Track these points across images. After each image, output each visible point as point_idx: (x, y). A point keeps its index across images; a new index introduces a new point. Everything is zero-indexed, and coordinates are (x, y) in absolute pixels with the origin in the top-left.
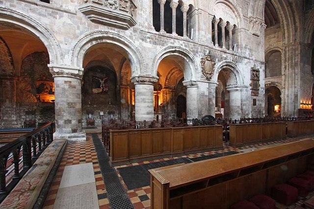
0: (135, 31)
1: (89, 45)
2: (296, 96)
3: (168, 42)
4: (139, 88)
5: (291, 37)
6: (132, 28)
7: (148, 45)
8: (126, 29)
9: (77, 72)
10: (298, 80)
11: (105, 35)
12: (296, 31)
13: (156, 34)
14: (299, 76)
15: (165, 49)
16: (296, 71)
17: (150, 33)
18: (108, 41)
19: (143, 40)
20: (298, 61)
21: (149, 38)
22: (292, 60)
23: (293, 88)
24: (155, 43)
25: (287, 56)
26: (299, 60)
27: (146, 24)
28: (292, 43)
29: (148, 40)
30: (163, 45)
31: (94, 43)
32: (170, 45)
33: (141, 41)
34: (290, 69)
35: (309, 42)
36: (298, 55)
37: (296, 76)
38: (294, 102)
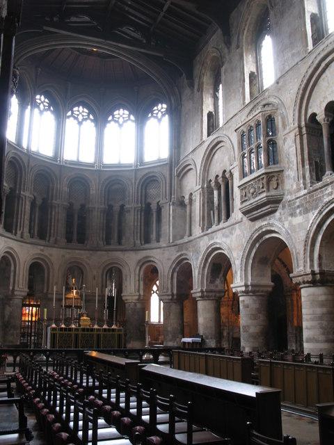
0: (284, 207)
1: (254, 251)
3: (323, 196)
4: (305, 293)
6: (281, 206)
7: (298, 220)
8: (276, 210)
9: (243, 289)
11: (260, 232)
13: (305, 195)
15: (320, 212)
17: (298, 198)
18: (267, 236)
19: (292, 215)
21: (298, 207)
24: (307, 211)
27: (295, 187)
29: (298, 211)
30: (316, 208)
31: (257, 246)
32: (327, 199)
33: (290, 218)
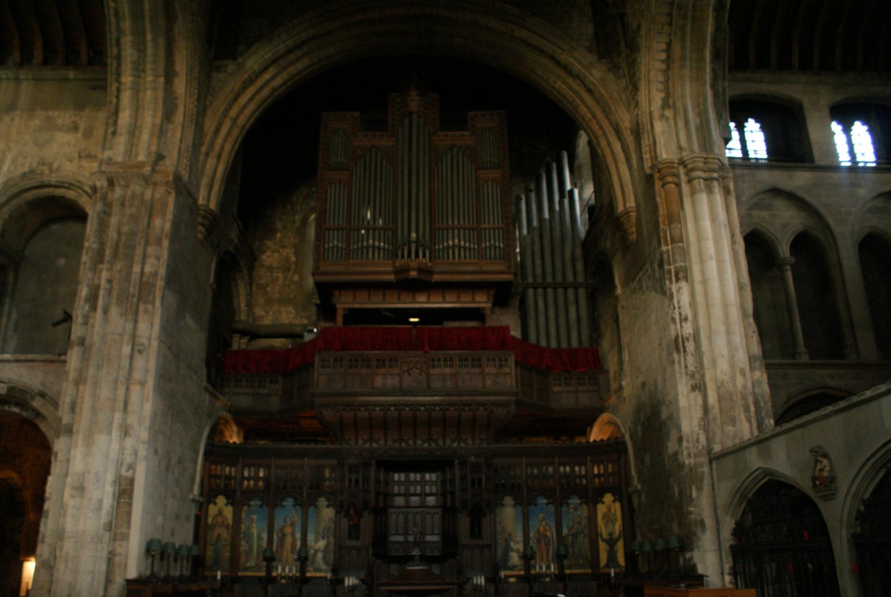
2: (124, 491)
5: (145, 137)
10: (143, 384)
12: (168, 115)
14: (152, 366)
16: (143, 326)
20: (155, 274)
22: (130, 259)
23: (115, 434)
25: (112, 234)
26: (162, 272)
28: (141, 165)
34: (114, 311)
35: (213, 206)
36: (159, 242)
37: (139, 362)
38: (109, 527)
